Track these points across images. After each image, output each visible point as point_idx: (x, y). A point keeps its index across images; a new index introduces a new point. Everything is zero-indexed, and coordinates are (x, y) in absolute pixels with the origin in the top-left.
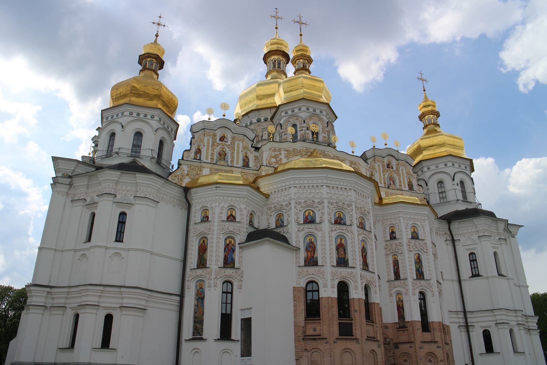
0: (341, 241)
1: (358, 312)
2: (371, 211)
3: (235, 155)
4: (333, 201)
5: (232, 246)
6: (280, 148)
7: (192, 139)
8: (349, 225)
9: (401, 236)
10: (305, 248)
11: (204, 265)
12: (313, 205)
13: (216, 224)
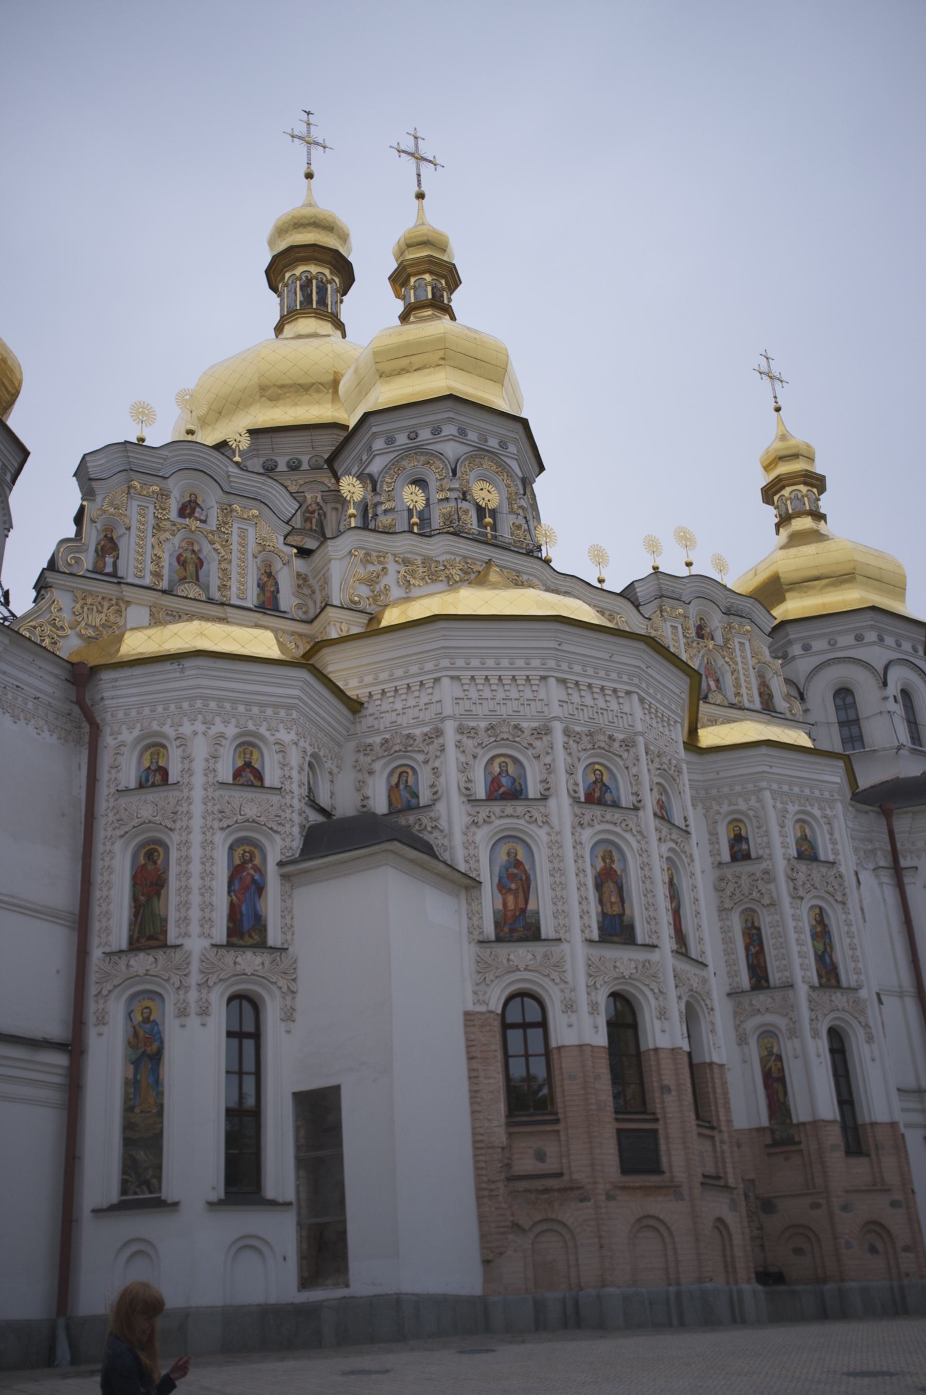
0: (608, 861)
1: (673, 1093)
2: (684, 766)
3: (234, 569)
4: (578, 729)
5: (252, 872)
6: (380, 552)
7: (85, 503)
8: (632, 807)
9: (767, 851)
10: (496, 880)
11: (157, 939)
12: (517, 739)
13: (198, 794)
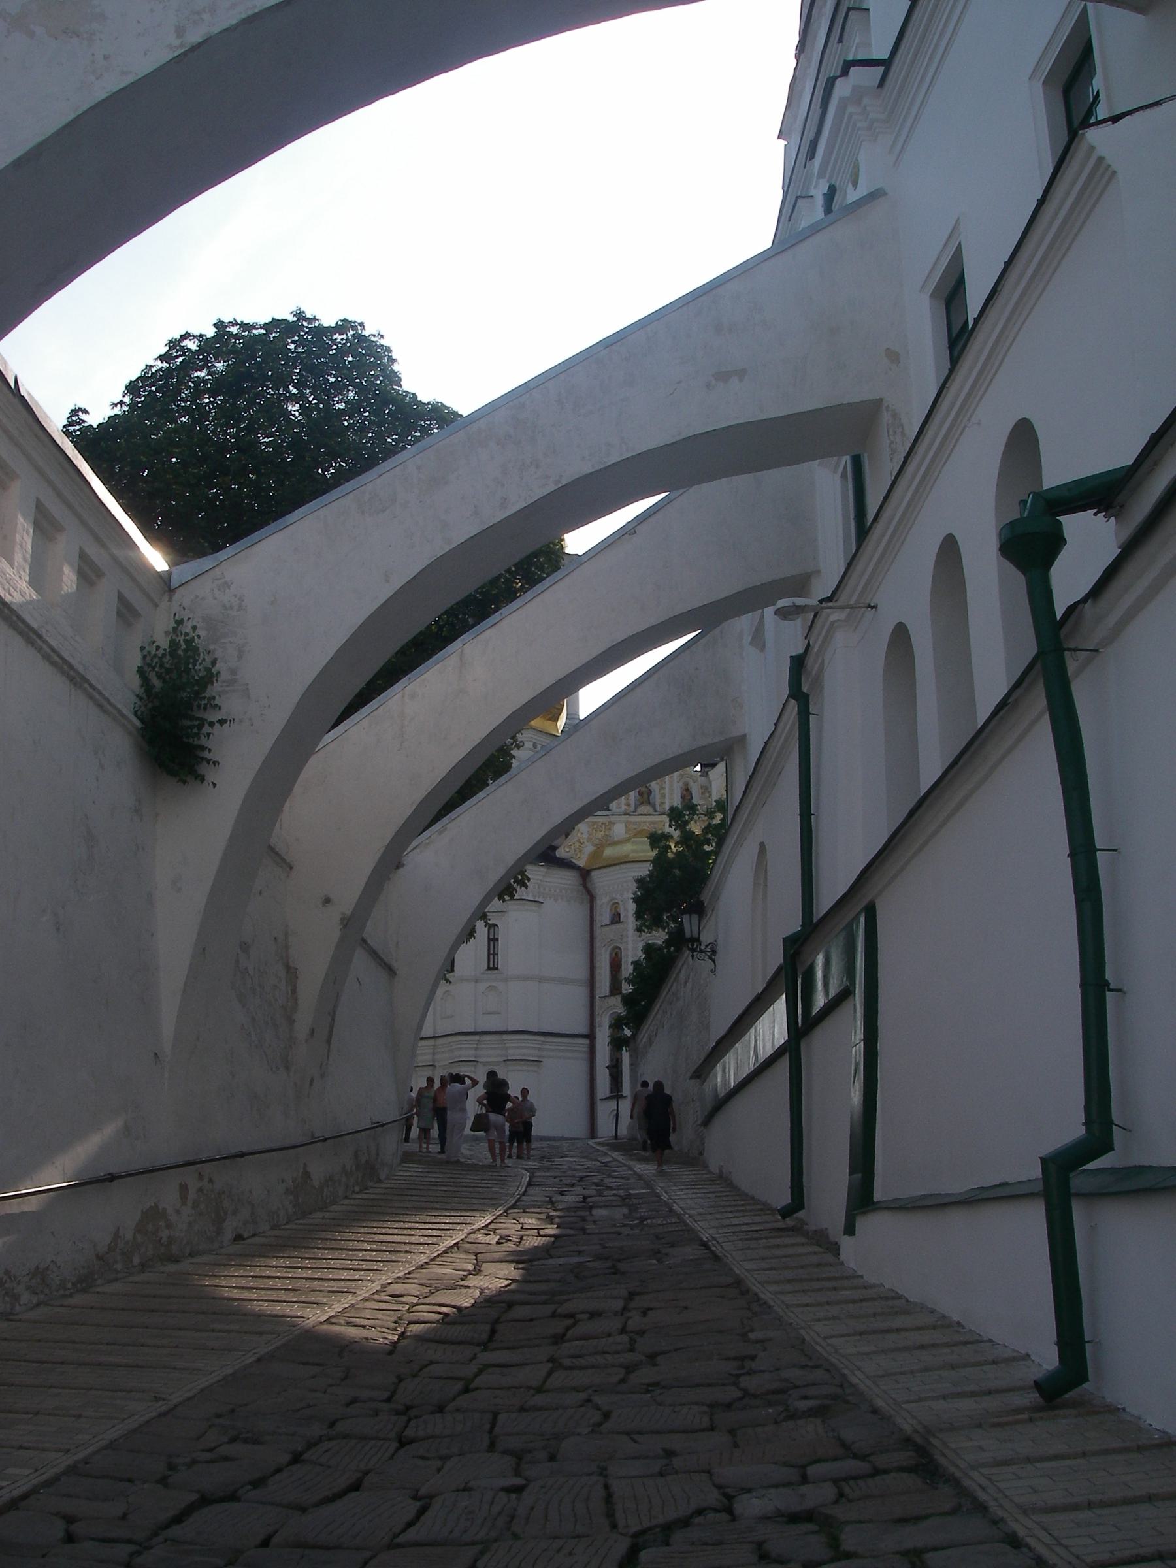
3: (667, 791)
